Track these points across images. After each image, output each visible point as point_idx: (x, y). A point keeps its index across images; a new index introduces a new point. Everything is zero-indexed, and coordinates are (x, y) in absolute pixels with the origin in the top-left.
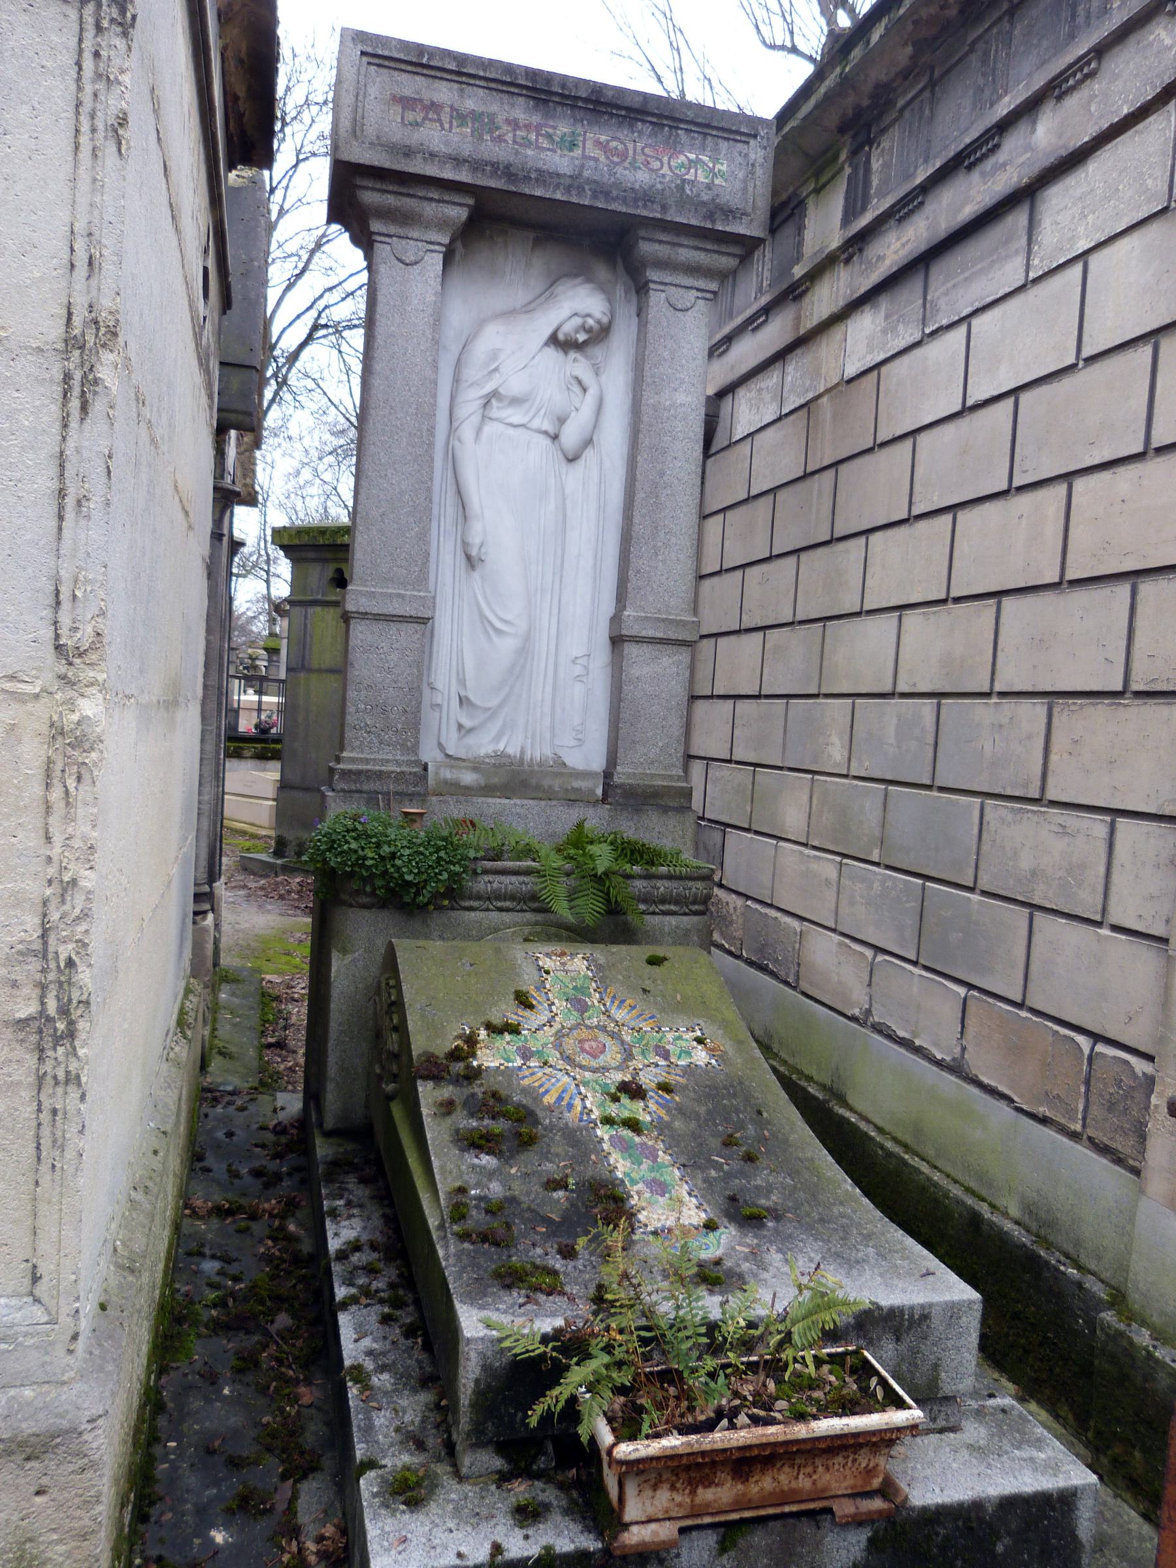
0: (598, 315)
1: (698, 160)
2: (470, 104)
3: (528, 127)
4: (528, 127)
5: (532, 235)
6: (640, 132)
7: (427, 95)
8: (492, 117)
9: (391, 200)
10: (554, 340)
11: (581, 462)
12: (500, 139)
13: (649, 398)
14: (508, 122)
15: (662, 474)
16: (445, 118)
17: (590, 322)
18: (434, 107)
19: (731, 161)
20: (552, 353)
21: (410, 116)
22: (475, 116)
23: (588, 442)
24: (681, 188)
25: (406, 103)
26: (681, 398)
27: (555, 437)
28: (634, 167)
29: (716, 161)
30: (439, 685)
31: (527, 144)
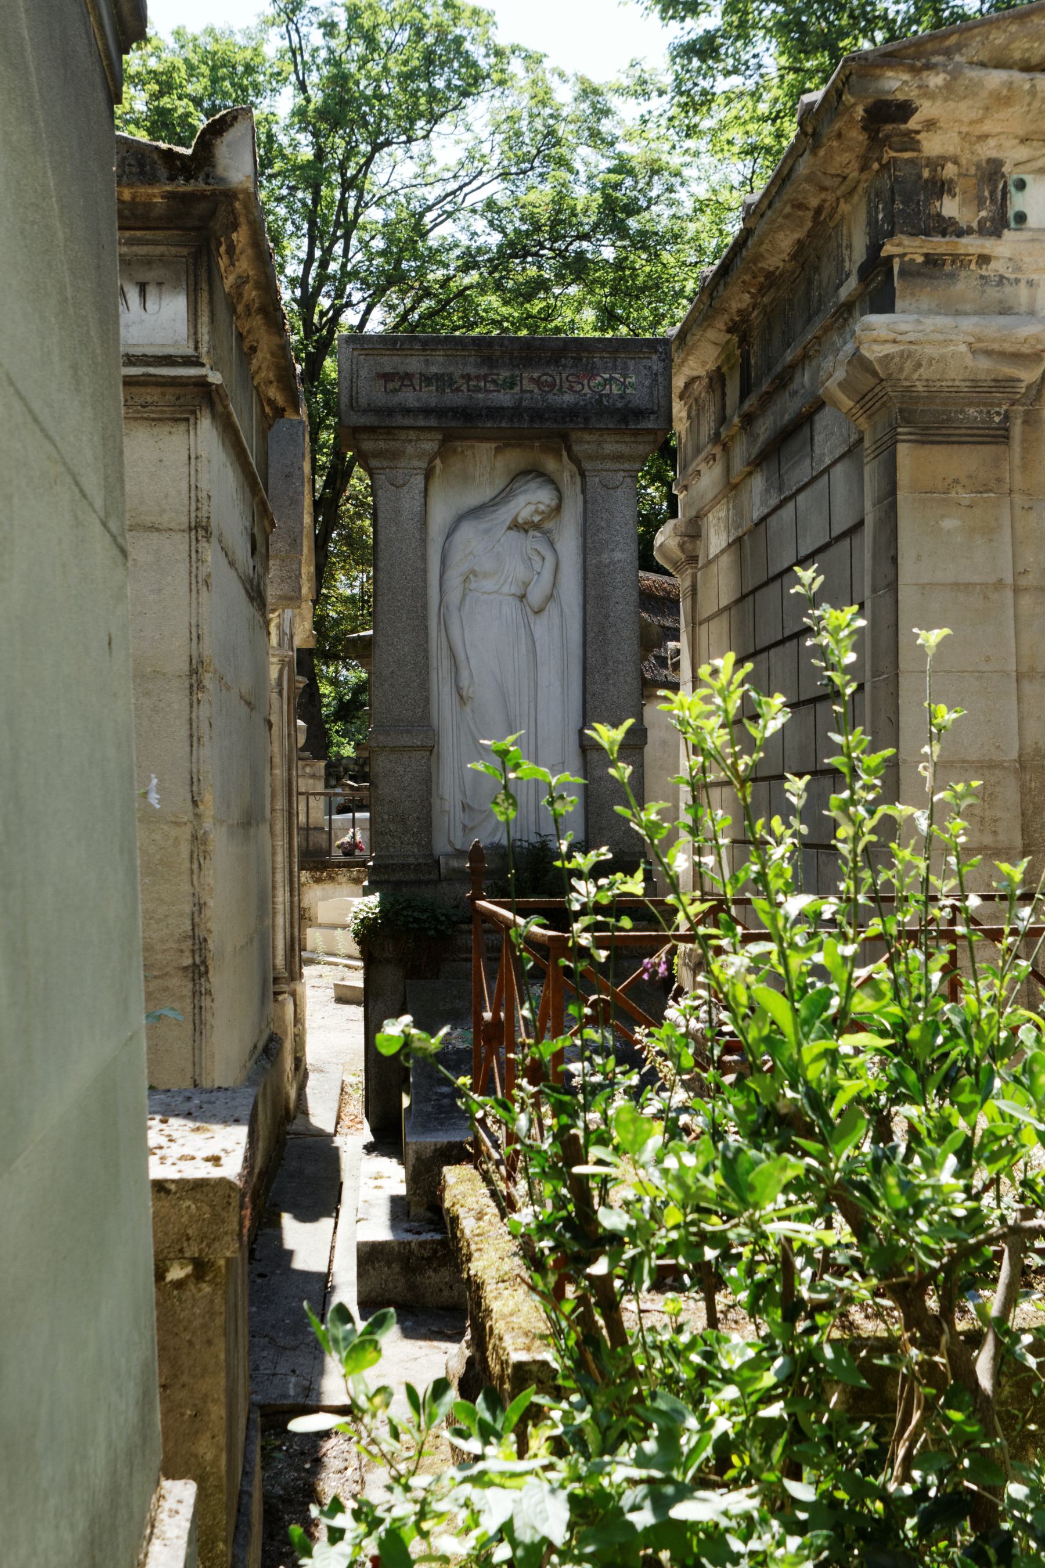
0: (547, 501)
1: (612, 378)
2: (434, 369)
3: (478, 378)
4: (478, 378)
5: (494, 445)
6: (564, 366)
7: (402, 369)
8: (450, 376)
9: (382, 445)
10: (515, 526)
11: (546, 613)
12: (458, 390)
13: (592, 561)
14: (463, 377)
15: (607, 616)
16: (416, 382)
17: (542, 507)
18: (408, 376)
19: (638, 374)
20: (513, 533)
21: (391, 386)
22: (438, 377)
23: (550, 597)
24: (599, 401)
25: (387, 377)
26: (618, 555)
27: (522, 597)
28: (561, 391)
29: (625, 376)
30: (446, 796)
31: (478, 390)
